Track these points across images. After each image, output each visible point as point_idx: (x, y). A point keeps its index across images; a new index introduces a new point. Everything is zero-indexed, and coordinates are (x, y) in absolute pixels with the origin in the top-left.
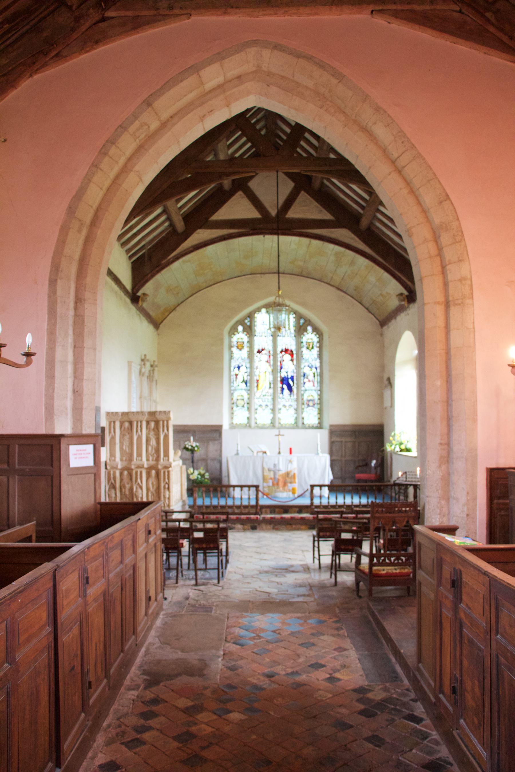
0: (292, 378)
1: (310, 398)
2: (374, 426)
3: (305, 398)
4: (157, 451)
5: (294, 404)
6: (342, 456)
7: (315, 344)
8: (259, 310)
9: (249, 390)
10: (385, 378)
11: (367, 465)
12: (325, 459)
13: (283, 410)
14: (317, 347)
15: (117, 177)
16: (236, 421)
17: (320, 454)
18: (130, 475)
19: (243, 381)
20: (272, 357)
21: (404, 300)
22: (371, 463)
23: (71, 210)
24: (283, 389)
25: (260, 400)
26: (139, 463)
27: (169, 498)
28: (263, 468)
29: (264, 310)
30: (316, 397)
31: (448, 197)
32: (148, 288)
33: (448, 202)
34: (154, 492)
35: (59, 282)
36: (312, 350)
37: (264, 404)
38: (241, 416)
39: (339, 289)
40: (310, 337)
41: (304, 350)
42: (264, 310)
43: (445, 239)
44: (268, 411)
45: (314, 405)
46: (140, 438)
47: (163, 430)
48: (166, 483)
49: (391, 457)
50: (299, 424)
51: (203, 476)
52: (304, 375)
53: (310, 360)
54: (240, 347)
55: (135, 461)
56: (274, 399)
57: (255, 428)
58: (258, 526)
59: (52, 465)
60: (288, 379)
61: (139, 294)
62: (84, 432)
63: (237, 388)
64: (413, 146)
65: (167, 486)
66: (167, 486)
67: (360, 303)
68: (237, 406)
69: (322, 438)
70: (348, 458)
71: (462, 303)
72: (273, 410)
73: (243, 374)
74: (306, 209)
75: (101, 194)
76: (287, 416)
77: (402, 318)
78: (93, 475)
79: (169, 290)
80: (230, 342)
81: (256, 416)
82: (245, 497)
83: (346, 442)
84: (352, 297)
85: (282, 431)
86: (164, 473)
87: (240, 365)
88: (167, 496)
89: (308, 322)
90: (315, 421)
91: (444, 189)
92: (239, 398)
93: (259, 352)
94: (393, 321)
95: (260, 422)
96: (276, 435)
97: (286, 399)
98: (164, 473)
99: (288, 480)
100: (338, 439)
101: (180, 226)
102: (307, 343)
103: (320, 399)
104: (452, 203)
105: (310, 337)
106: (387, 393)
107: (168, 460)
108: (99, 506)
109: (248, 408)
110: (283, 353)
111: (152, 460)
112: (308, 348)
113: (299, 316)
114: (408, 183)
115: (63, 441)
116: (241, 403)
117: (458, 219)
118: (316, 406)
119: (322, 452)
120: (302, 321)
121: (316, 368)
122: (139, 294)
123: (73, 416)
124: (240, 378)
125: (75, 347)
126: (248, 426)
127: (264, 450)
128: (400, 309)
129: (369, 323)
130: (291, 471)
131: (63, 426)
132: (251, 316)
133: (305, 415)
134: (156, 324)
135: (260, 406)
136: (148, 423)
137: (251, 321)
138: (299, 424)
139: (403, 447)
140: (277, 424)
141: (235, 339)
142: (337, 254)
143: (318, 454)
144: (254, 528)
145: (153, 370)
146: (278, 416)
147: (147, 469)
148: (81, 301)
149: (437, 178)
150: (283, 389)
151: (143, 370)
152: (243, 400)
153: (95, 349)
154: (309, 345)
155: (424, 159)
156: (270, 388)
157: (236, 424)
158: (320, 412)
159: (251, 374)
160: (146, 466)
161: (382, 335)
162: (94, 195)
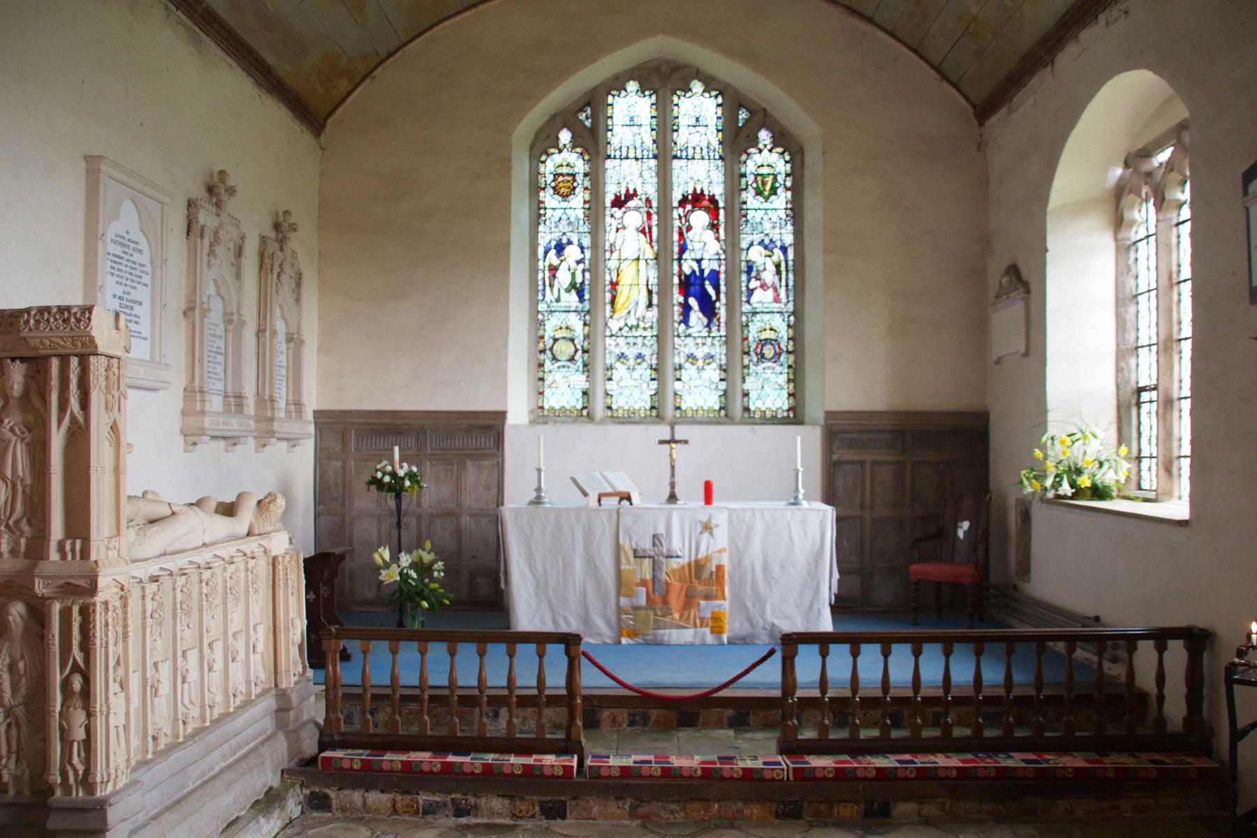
0: (715, 276)
1: (768, 335)
2: (959, 415)
3: (753, 333)
5: (719, 350)
6: (862, 506)
7: (780, 179)
8: (617, 84)
10: (996, 267)
11: (943, 534)
12: (819, 521)
13: (689, 372)
14: (787, 189)
17: (805, 504)
19: (573, 285)
20: (654, 217)
22: (956, 528)
24: (686, 309)
25: (621, 341)
27: (88, 744)
28: (618, 548)
29: (632, 86)
30: (784, 333)
34: (20, 711)
36: (773, 197)
37: (631, 353)
38: (565, 388)
40: (766, 159)
41: (749, 196)
42: (632, 86)
44: (644, 372)
45: (778, 355)
48: (76, 668)
49: (1026, 516)
50: (733, 411)
51: (423, 569)
54: (564, 189)
56: (660, 338)
57: (603, 421)
58: (570, 804)
60: (702, 279)
65: (77, 683)
66: (77, 683)
67: (915, 51)
68: (555, 359)
69: (803, 448)
73: (571, 264)
76: (699, 390)
80: (535, 175)
81: (610, 386)
83: (874, 463)
84: (891, 34)
85: (681, 432)
86: (66, 615)
87: (564, 241)
88: (80, 734)
92: (559, 335)
93: (618, 203)
95: (621, 402)
96: (662, 442)
97: (697, 339)
99: (700, 588)
100: (850, 455)
102: (756, 176)
103: (797, 337)
105: (766, 159)
107: (85, 553)
109: (585, 365)
110: (689, 207)
111: (14, 552)
112: (759, 193)
113: (732, 100)
116: (564, 349)
118: (783, 358)
119: (807, 497)
120: (743, 115)
121: (784, 249)
124: (564, 278)
126: (585, 414)
127: (621, 488)
130: (708, 559)
132: (595, 100)
134: (311, 114)
135: (622, 357)
138: (733, 411)
139: (1084, 481)
140: (669, 412)
141: (549, 166)
143: (796, 503)
144: (555, 811)
150: (686, 309)
152: (572, 340)
154: (764, 184)
156: (650, 305)
157: (552, 409)
158: (796, 377)
159: (595, 266)
161: (981, 145)
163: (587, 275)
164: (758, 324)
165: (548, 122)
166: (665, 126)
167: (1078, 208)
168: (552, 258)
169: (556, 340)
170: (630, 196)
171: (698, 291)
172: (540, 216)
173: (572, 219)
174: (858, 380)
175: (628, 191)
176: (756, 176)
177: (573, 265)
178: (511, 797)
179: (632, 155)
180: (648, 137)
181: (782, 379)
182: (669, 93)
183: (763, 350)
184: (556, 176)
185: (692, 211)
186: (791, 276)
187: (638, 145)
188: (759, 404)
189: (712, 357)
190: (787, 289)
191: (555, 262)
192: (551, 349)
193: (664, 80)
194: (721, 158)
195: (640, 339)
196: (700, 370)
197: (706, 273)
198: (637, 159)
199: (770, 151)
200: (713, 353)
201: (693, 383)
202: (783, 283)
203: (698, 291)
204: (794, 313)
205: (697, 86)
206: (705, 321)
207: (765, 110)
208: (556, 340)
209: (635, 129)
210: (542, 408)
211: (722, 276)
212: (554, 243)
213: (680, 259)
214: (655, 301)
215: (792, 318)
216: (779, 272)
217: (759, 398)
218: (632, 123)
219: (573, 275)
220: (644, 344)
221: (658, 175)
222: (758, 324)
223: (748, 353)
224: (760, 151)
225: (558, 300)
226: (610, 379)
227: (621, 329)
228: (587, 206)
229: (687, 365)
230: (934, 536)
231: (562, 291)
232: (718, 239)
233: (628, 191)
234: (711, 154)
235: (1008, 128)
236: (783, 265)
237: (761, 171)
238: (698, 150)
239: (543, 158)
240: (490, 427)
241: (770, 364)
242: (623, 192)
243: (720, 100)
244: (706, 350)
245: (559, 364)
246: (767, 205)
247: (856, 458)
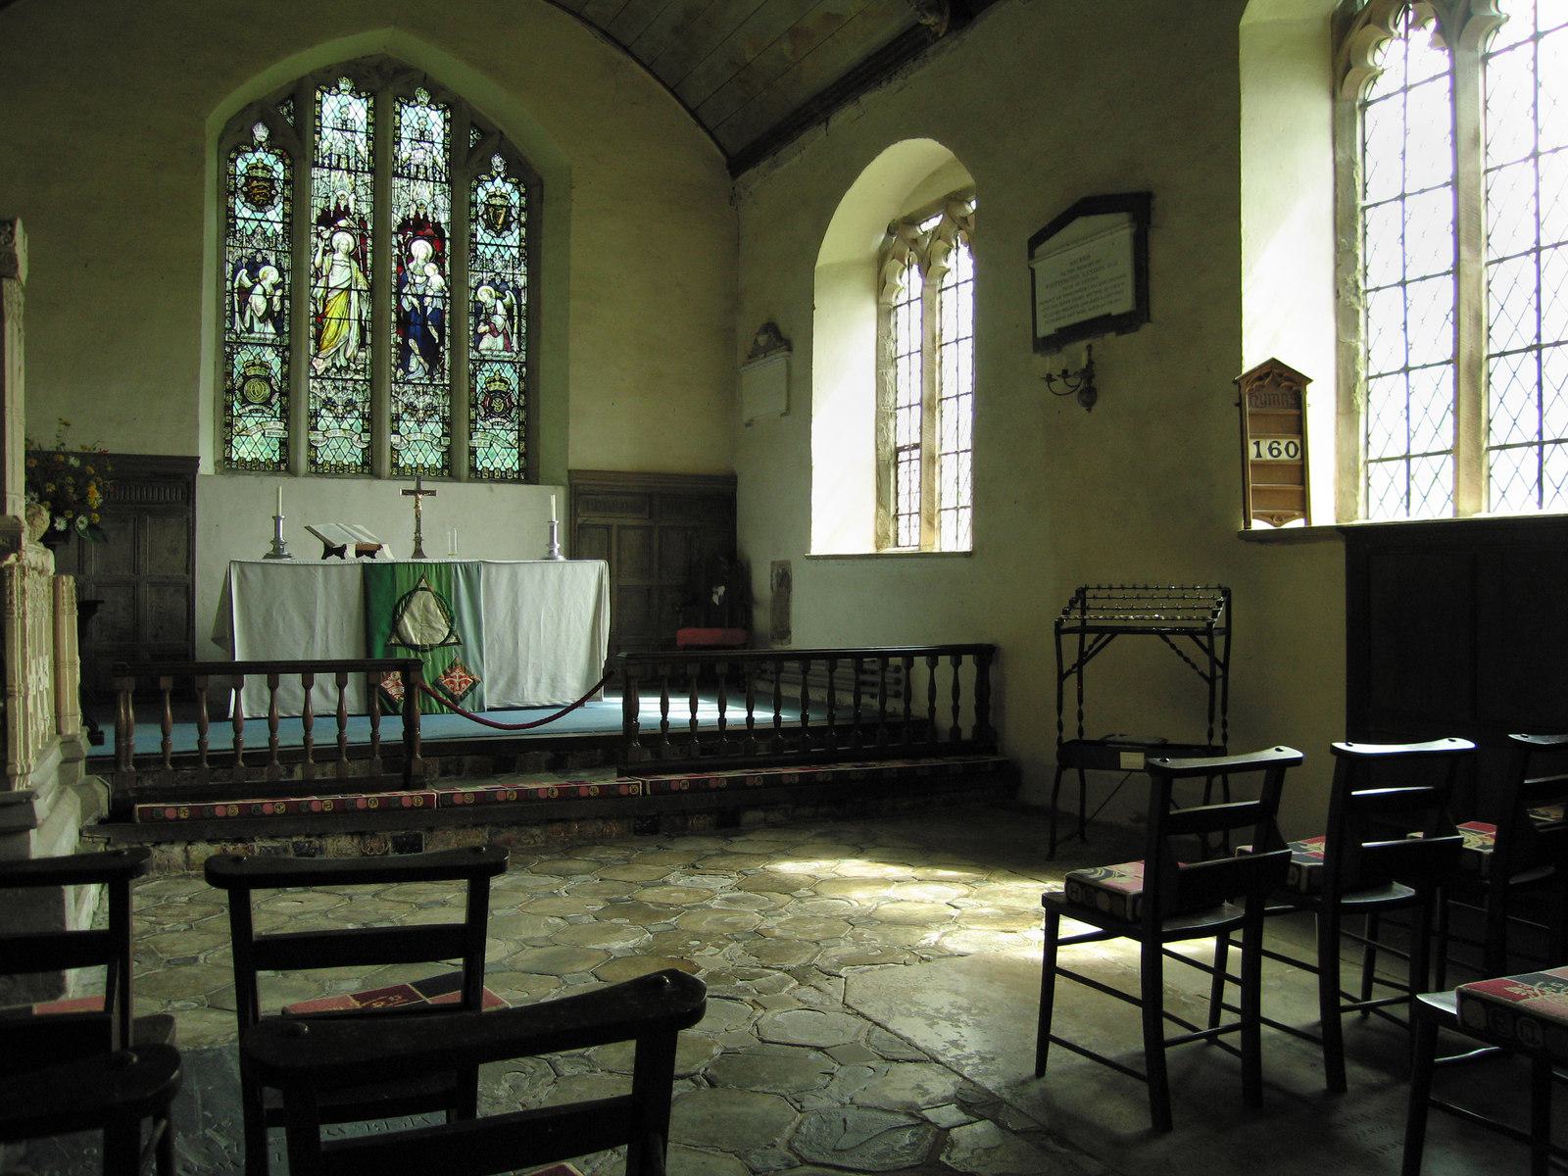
0: (439, 314)
5: (441, 402)
9: (288, 348)
13: (408, 424)
14: (521, 225)
20: (369, 242)
25: (328, 384)
36: (506, 233)
37: (340, 398)
38: (256, 441)
39: (607, 35)
40: (498, 188)
44: (353, 422)
53: (499, 264)
54: (260, 194)
56: (374, 384)
67: (672, 91)
72: (372, 422)
80: (226, 175)
81: (315, 436)
83: (621, 528)
87: (259, 258)
92: (251, 372)
93: (328, 219)
95: (326, 455)
96: (406, 493)
102: (488, 206)
110: (410, 234)
112: (490, 226)
120: (474, 136)
121: (517, 291)
133: (478, 440)
150: (405, 353)
152: (268, 379)
154: (496, 216)
156: (362, 345)
161: (733, 198)
163: (287, 303)
164: (487, 374)
165: (243, 111)
166: (383, 133)
167: (843, 271)
169: (246, 378)
170: (343, 213)
172: (229, 226)
173: (269, 234)
174: (606, 436)
175: (338, 205)
176: (488, 206)
177: (269, 290)
178: (361, 834)
179: (343, 165)
181: (512, 437)
182: (390, 97)
183: (492, 404)
184: (249, 179)
185: (414, 239)
186: (524, 322)
187: (352, 154)
188: (487, 463)
189: (435, 408)
190: (519, 338)
191: (248, 283)
192: (241, 389)
194: (448, 181)
195: (350, 384)
196: (419, 422)
197: (429, 310)
198: (349, 171)
199: (504, 180)
200: (435, 403)
201: (412, 437)
202: (515, 331)
204: (525, 364)
205: (423, 97)
206: (427, 366)
207: (501, 133)
208: (246, 378)
209: (348, 135)
210: (230, 459)
211: (447, 316)
212: (244, 260)
213: (399, 294)
214: (369, 340)
215: (524, 369)
216: (510, 317)
217: (487, 457)
218: (344, 127)
219: (270, 302)
220: (355, 390)
221: (374, 193)
222: (487, 374)
223: (475, 406)
224: (493, 179)
225: (250, 330)
226: (314, 428)
227: (327, 370)
228: (287, 220)
229: (405, 416)
231: (255, 320)
232: (442, 273)
233: (338, 205)
234: (438, 176)
235: (768, 183)
236: (515, 307)
237: (493, 201)
238: (422, 170)
239: (233, 155)
240: (179, 474)
241: (499, 419)
242: (332, 208)
243: (448, 115)
244: (428, 399)
245: (251, 407)
246: (499, 241)
247: (603, 521)
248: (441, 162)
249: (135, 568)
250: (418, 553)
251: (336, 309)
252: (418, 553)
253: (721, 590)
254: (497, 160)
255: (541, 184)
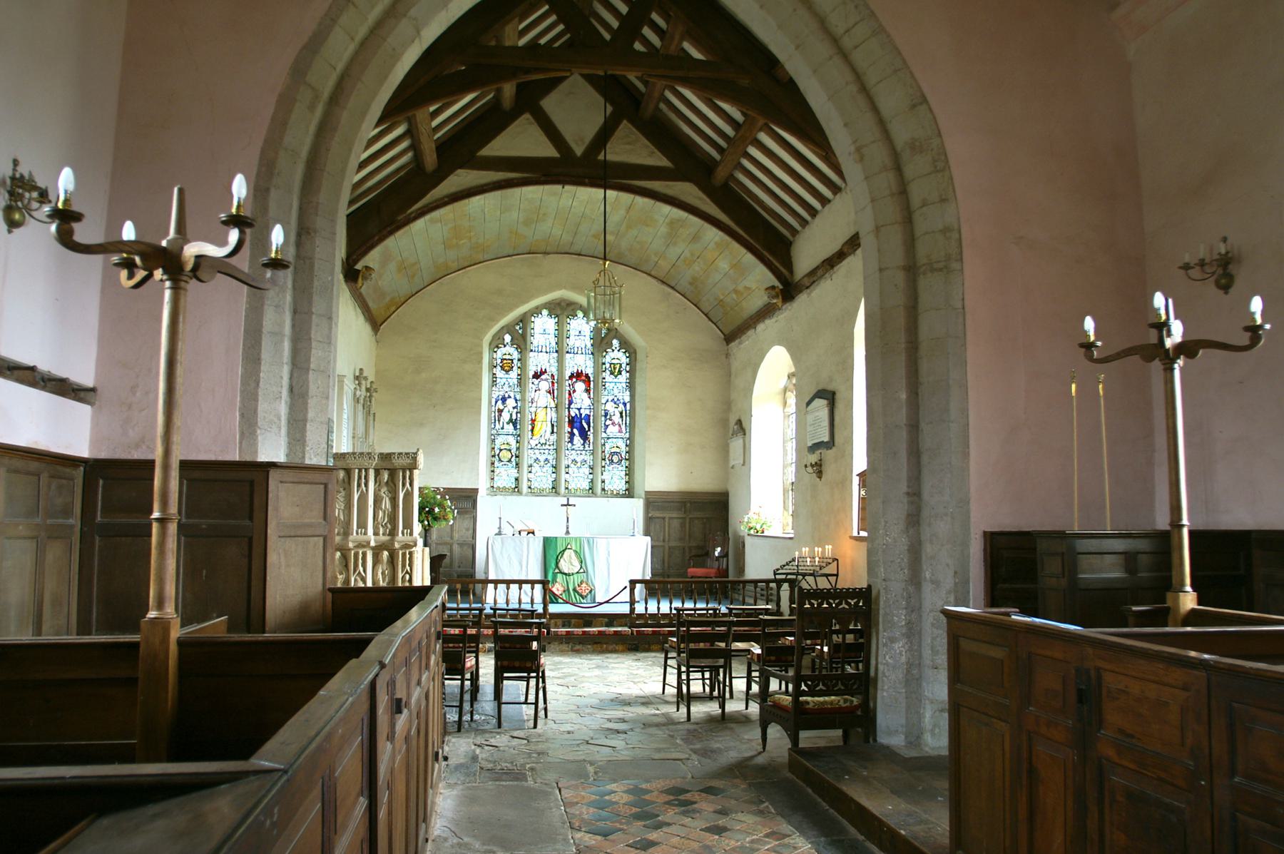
2: (713, 494)
4: (393, 519)
5: (589, 458)
8: (537, 311)
10: (733, 420)
13: (573, 469)
15: (379, 24)
16: (499, 483)
18: (345, 557)
19: (511, 420)
21: (776, 296)
23: (299, 71)
24: (572, 435)
26: (361, 538)
30: (624, 449)
31: (924, 100)
32: (372, 259)
33: (924, 107)
35: (274, 195)
37: (542, 458)
38: (506, 475)
39: (663, 282)
40: (616, 356)
42: (545, 312)
43: (915, 167)
44: (548, 468)
46: (363, 498)
47: (404, 485)
52: (606, 415)
54: (507, 366)
55: (355, 536)
59: (251, 518)
61: (359, 266)
62: (307, 462)
63: (501, 431)
64: (873, 14)
70: (673, 544)
71: (946, 267)
74: (630, 148)
75: (352, 48)
76: (578, 478)
77: (766, 328)
78: (321, 539)
79: (403, 267)
82: (526, 599)
86: (404, 555)
89: (613, 333)
90: (620, 485)
91: (919, 87)
93: (537, 376)
94: (751, 332)
97: (576, 452)
98: (404, 555)
100: (657, 514)
101: (430, 160)
104: (931, 110)
105: (616, 356)
106: (736, 444)
108: (330, 595)
112: (612, 373)
114: (858, 77)
115: (274, 476)
116: (505, 455)
117: (940, 135)
121: (625, 404)
122: (359, 266)
123: (289, 433)
124: (506, 417)
125: (295, 312)
128: (766, 312)
129: (707, 336)
131: (272, 449)
132: (524, 320)
133: (606, 476)
134: (375, 323)
136: (377, 472)
137: (524, 328)
141: (500, 353)
142: (673, 224)
145: (370, 397)
146: (564, 476)
147: (373, 548)
148: (308, 233)
149: (908, 68)
150: (572, 435)
151: (358, 393)
153: (330, 318)
155: (888, 36)
158: (630, 472)
160: (373, 544)
161: (727, 355)
162: (340, 48)
166: (561, 336)
168: (500, 405)
170: (543, 373)
171: (579, 426)
174: (663, 473)
180: (553, 341)
184: (502, 360)
191: (501, 407)
193: (562, 310)
203: (579, 426)
205: (580, 314)
230: (702, 555)
248: (589, 346)
249: (452, 538)
250: (568, 532)
251: (541, 416)
252: (568, 532)
253: (719, 549)
254: (615, 342)
255: (635, 352)
